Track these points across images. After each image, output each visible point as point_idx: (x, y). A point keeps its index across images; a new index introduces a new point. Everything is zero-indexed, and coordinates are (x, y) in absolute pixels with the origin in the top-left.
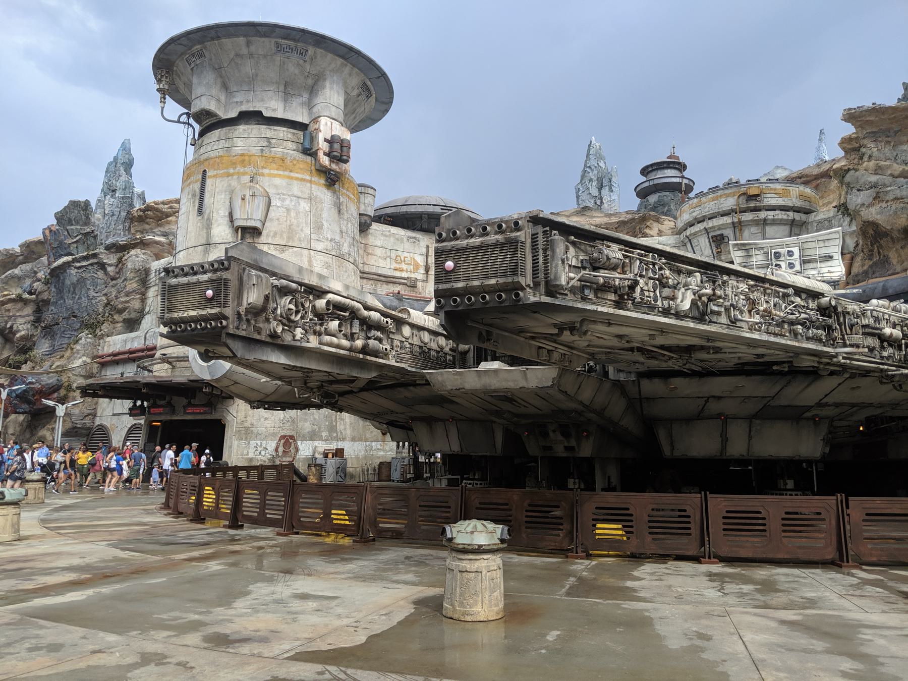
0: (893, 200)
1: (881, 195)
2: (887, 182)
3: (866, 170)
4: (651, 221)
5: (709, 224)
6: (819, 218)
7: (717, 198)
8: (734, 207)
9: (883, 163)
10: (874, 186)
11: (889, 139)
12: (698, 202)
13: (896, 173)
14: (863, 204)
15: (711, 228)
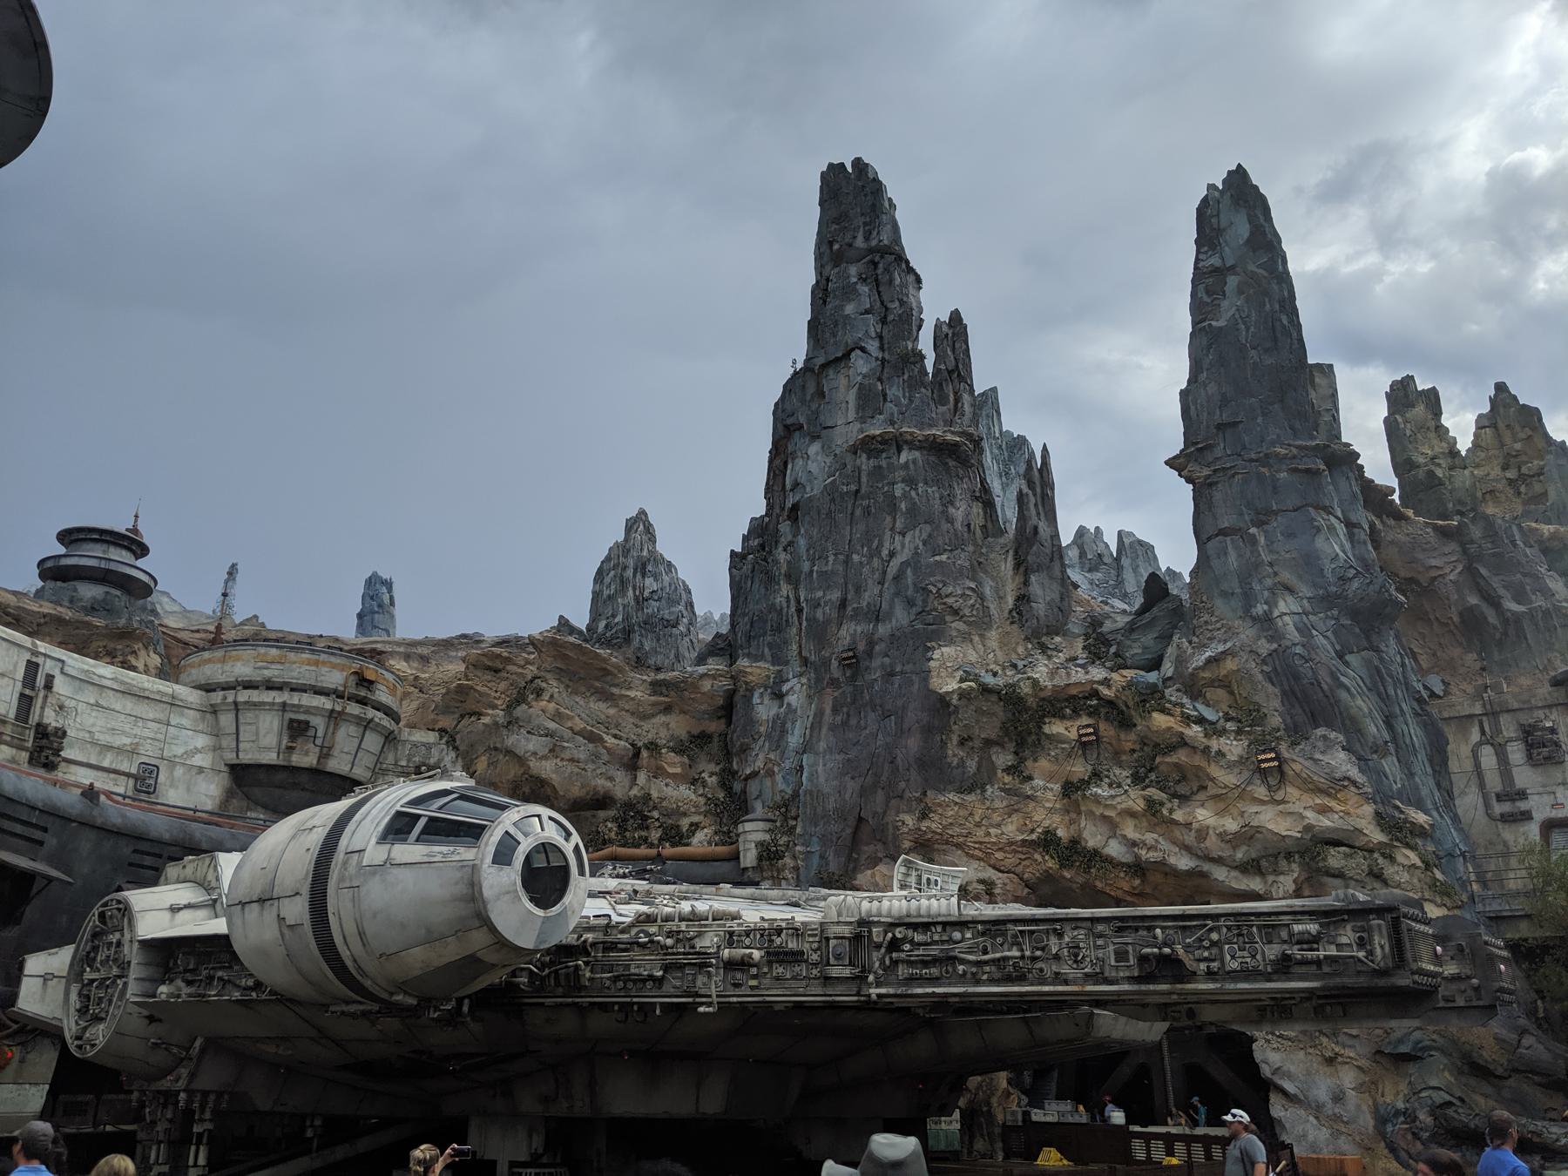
0: (569, 760)
1: (557, 748)
2: (566, 737)
3: (542, 710)
4: (141, 645)
5: (295, 699)
6: (414, 739)
7: (317, 663)
8: (341, 688)
10: (549, 734)
11: (571, 684)
12: (281, 657)
13: (577, 729)
14: (535, 754)
15: (294, 706)
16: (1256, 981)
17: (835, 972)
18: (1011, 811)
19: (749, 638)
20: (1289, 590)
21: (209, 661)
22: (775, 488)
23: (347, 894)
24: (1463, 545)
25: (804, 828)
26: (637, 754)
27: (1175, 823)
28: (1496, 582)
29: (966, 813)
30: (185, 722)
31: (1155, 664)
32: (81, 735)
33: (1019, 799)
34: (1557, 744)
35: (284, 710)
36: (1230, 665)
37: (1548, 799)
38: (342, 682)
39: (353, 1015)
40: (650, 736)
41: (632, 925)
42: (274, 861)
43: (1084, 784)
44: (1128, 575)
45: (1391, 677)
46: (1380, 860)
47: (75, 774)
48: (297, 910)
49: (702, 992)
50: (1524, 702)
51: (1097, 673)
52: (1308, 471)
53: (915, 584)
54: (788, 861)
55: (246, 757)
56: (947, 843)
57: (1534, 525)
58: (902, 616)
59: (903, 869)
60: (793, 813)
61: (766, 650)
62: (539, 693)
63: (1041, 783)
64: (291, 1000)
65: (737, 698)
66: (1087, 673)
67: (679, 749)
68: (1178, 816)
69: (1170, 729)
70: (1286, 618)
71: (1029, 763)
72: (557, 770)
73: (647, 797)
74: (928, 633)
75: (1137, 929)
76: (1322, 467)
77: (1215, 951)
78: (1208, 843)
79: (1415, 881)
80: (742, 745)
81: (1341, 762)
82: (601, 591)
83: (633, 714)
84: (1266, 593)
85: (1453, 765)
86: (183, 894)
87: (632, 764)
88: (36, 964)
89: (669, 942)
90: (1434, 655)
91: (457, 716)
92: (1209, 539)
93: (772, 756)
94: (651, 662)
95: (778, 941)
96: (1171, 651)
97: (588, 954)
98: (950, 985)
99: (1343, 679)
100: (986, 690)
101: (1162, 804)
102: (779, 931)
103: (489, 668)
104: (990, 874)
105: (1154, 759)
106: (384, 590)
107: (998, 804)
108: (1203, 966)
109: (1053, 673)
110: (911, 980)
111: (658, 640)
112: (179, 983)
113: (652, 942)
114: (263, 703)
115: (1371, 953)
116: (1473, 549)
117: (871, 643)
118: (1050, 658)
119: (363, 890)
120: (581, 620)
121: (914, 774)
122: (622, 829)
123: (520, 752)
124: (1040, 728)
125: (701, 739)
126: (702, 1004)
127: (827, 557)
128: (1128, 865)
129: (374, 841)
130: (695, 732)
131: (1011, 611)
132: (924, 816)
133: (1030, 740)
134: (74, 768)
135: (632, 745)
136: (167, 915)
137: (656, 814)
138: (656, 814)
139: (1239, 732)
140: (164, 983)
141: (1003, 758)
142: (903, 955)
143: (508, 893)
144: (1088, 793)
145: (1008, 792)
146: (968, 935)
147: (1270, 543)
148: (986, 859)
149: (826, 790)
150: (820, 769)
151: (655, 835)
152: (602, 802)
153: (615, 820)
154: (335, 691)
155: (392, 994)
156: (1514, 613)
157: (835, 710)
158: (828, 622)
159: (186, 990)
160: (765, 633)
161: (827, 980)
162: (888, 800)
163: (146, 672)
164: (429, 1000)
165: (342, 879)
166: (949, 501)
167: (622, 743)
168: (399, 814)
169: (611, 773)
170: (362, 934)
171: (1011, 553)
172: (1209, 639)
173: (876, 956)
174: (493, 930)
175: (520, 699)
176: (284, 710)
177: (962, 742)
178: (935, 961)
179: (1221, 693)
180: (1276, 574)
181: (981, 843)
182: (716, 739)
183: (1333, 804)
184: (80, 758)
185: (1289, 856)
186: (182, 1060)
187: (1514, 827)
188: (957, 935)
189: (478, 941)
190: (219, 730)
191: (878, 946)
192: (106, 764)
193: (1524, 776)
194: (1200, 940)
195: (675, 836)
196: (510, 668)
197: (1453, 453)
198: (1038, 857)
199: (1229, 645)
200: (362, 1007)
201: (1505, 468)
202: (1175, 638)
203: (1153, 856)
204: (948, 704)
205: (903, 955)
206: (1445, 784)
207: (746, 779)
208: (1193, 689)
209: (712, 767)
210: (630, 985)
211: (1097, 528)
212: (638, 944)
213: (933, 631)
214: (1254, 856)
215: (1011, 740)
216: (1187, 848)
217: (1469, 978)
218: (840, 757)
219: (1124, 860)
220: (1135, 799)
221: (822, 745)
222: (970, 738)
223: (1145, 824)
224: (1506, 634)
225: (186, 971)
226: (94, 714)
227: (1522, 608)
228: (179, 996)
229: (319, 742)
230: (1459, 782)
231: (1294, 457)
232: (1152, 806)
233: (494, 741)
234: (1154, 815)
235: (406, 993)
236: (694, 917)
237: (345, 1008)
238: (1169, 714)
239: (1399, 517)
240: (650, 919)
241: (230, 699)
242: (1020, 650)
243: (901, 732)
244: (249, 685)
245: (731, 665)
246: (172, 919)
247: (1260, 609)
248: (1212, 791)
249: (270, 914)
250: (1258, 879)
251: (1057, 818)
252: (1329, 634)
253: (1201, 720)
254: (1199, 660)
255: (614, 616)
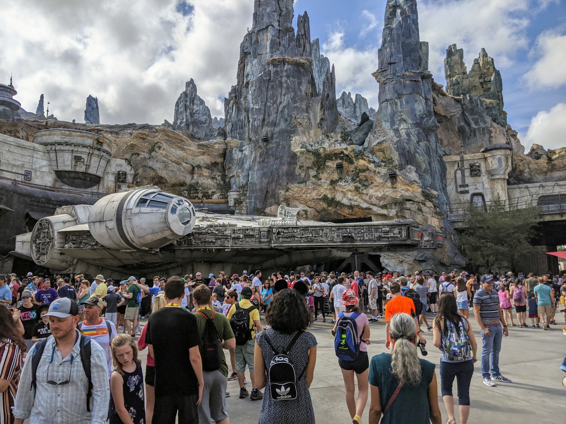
7: (82, 136)
9: (168, 154)
13: (173, 160)
15: (76, 151)
16: (372, 242)
17: (263, 240)
18: (314, 189)
19: (232, 130)
20: (405, 121)
21: (44, 135)
22: (241, 75)
23: (128, 221)
24: (462, 105)
25: (249, 194)
26: (193, 168)
27: (363, 194)
28: (470, 118)
29: (300, 190)
30: (39, 156)
31: (362, 143)
32: (5, 161)
33: (317, 186)
34: (479, 170)
35: (72, 153)
36: (385, 145)
37: (474, 187)
38: (92, 143)
39: (128, 253)
40: (198, 163)
41: (206, 228)
42: (103, 211)
43: (337, 181)
44: (358, 110)
45: (432, 149)
46: (422, 206)
47: (4, 175)
48: (112, 224)
49: (227, 245)
50: (471, 157)
51: (344, 146)
52: (415, 81)
53: (288, 114)
54: (244, 204)
55: (61, 168)
56: (294, 199)
57: (485, 99)
58: (283, 125)
59: (281, 209)
60: (246, 189)
61: (237, 135)
62: (160, 148)
63: (324, 181)
64: (107, 248)
65: (227, 151)
66: (341, 146)
67: (208, 167)
68: (364, 192)
69: (364, 165)
70: (403, 130)
71: (321, 175)
72: (167, 174)
73: (198, 183)
74: (291, 132)
75: (343, 229)
76: (420, 80)
77: (362, 234)
78: (372, 200)
79: (431, 211)
80: (229, 167)
81: (414, 176)
82: (178, 110)
83: (191, 155)
84: (398, 122)
85: (448, 176)
86: (66, 217)
87: (192, 172)
88: (19, 238)
89: (217, 232)
90: (449, 140)
91: (131, 154)
92: (383, 102)
93: (239, 171)
94: (197, 136)
95: (247, 232)
96: (367, 139)
97: (194, 236)
98: (293, 243)
99: (417, 150)
100: (308, 151)
101: (360, 188)
102: (248, 230)
103: (141, 138)
104: (306, 208)
105: (358, 174)
106: (94, 102)
107: (310, 187)
108: (359, 238)
109: (330, 146)
110: (283, 242)
111: (199, 128)
112: (71, 243)
113: (212, 232)
114: (65, 150)
115: (401, 235)
116: (464, 107)
117: (272, 135)
118: (329, 140)
119: (133, 220)
120: (171, 121)
121: (285, 178)
122: (189, 194)
123: (154, 168)
124: (325, 163)
125: (215, 164)
126: (226, 249)
127: (258, 103)
128: (348, 206)
129: (135, 206)
130: (213, 162)
131: (318, 124)
132: (287, 191)
133: (321, 167)
134: (4, 172)
135: (192, 166)
136: (62, 224)
137: (200, 188)
138: (200, 188)
139: (385, 166)
140: (66, 244)
141: (313, 173)
142: (281, 236)
143: (175, 221)
144: (338, 184)
145: (313, 183)
146: (299, 231)
147: (401, 105)
148: (306, 203)
149: (256, 182)
150: (255, 176)
151: (200, 195)
152: (182, 184)
153: (187, 190)
154: (90, 146)
155: (141, 247)
156: (474, 128)
157: (260, 156)
158: (258, 127)
159: (73, 246)
160: (237, 129)
161: (260, 242)
162: (276, 186)
163: (23, 139)
164: (152, 248)
165: (126, 216)
166: (300, 84)
167: (188, 165)
168: (141, 198)
169: (185, 175)
170: (133, 231)
171: (320, 103)
172: (380, 136)
173: (274, 236)
174: (171, 230)
175: (152, 150)
176: (72, 153)
177: (301, 167)
178: (289, 237)
179: (381, 153)
180: (402, 115)
181: (304, 199)
182: (220, 164)
183: (410, 188)
184: (5, 169)
185: (395, 204)
186: (70, 265)
187: (463, 195)
188: (296, 231)
189: (167, 234)
190: (50, 159)
191: (275, 233)
192: (14, 171)
193: (469, 180)
194: (359, 232)
195: (207, 196)
196: (148, 138)
197: (464, 73)
198: (321, 203)
199: (385, 138)
200: (131, 250)
201: (480, 78)
202: (369, 134)
203: (356, 203)
204: (296, 155)
205: (281, 236)
206: (444, 182)
207: (230, 178)
208: (373, 152)
209: (219, 174)
210: (206, 244)
211: (349, 93)
212: (208, 233)
213: (293, 130)
214: (385, 204)
215: (315, 167)
216: (365, 201)
217: (431, 241)
218: (261, 172)
219: (347, 204)
220: (351, 186)
221: (256, 168)
222: (303, 166)
223: (354, 194)
224: (470, 135)
225: (72, 240)
226: (8, 154)
227: (477, 127)
228: (71, 248)
229: (85, 163)
230: (448, 181)
231: (412, 76)
232: (357, 188)
233: (145, 163)
234: (357, 191)
235: (145, 247)
236: (224, 226)
237: (125, 251)
238: (365, 160)
239: (444, 95)
240: (211, 226)
241: (53, 148)
242: (320, 137)
243: (281, 164)
244: (59, 144)
245: (225, 140)
246: (64, 225)
247: (396, 126)
248: (375, 184)
249: (103, 226)
250: (386, 210)
251: (328, 192)
252: (415, 136)
253: (374, 162)
254: (375, 143)
255: (183, 119)
